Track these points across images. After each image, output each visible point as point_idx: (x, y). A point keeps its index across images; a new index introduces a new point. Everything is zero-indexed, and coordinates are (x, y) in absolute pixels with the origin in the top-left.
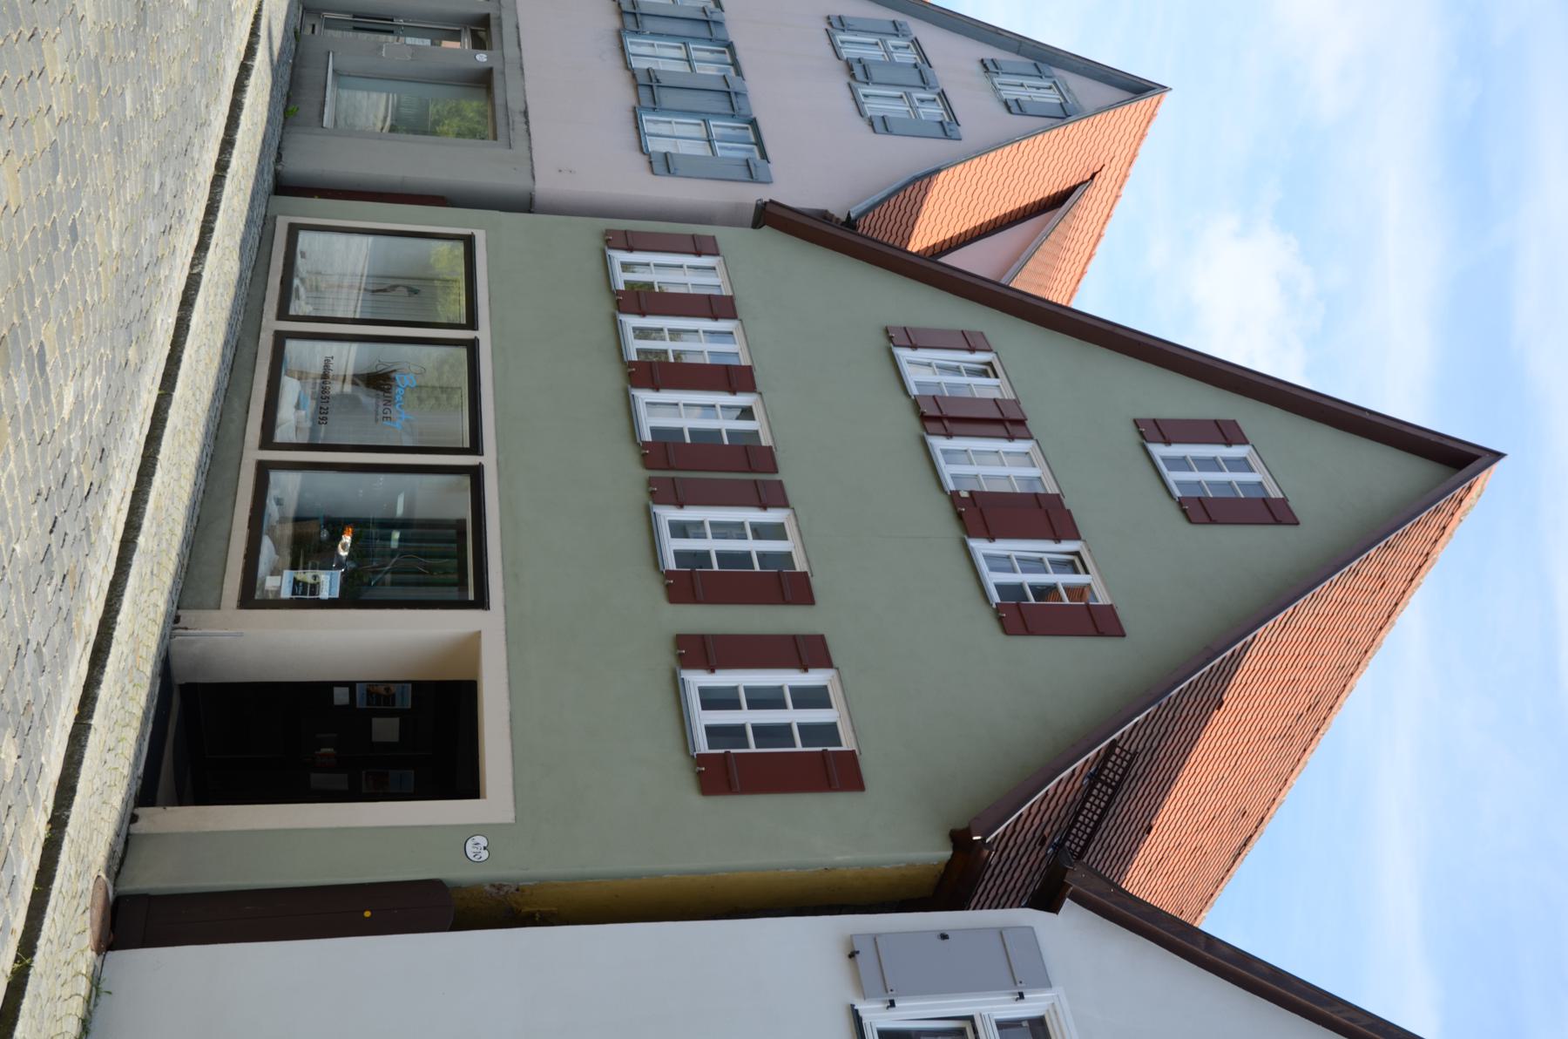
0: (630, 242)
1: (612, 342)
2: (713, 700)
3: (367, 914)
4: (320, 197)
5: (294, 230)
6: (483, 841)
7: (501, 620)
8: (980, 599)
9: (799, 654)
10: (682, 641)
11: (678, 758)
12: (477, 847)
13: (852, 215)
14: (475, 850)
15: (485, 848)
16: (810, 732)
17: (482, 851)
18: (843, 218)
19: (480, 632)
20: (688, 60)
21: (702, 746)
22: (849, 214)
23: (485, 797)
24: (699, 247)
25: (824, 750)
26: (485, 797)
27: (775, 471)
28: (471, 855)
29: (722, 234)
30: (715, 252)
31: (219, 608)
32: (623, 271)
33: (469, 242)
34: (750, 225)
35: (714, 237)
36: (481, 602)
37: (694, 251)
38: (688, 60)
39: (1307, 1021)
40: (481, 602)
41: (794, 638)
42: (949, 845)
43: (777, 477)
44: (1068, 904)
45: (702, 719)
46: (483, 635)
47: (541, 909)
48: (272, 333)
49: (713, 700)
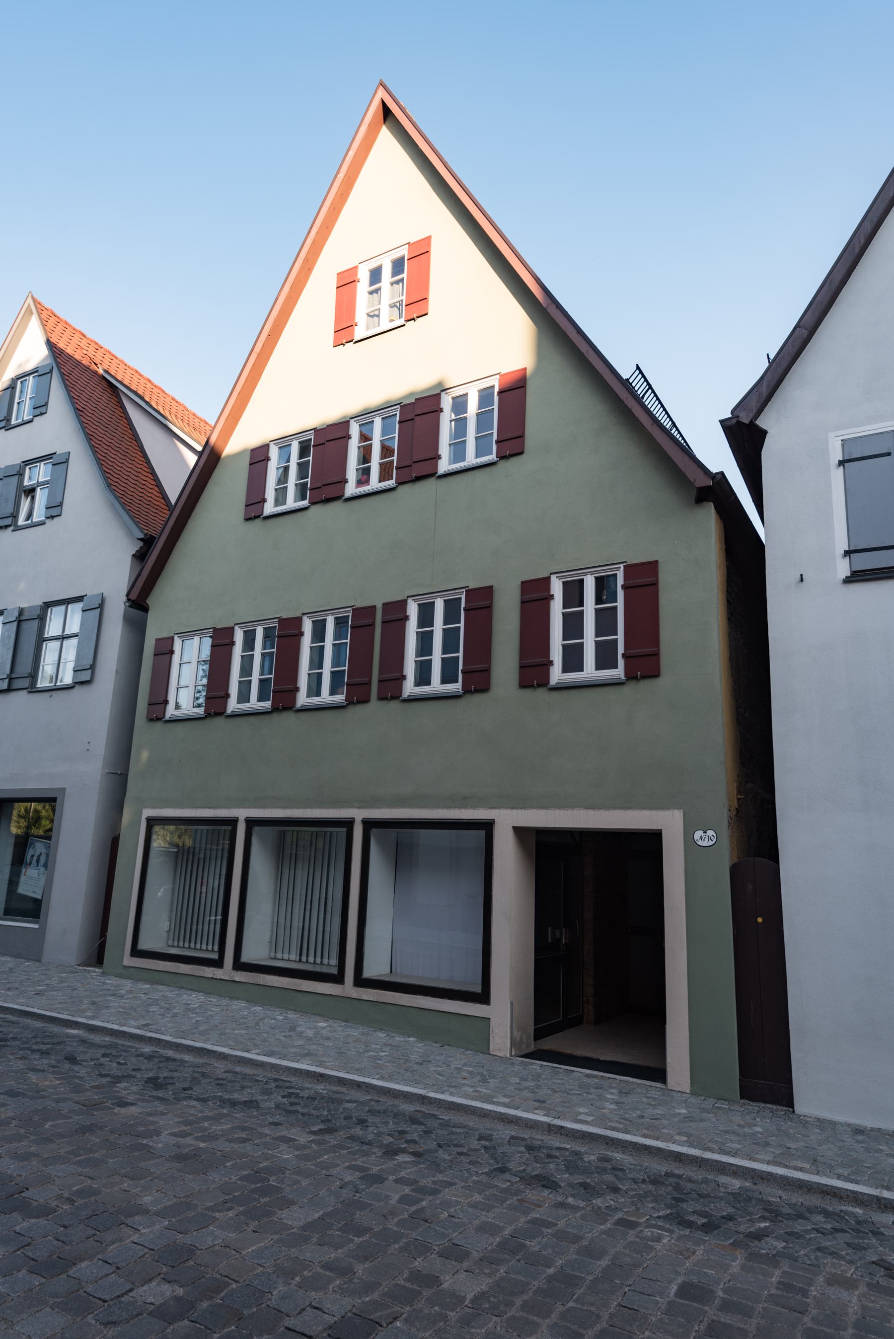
0: (159, 701)
1: (252, 719)
2: (423, 677)
3: (760, 920)
4: (106, 931)
5: (136, 952)
6: (698, 834)
7: (504, 812)
8: (493, 468)
9: (530, 601)
10: (525, 683)
11: (627, 690)
12: (704, 838)
13: (142, 536)
14: (707, 839)
15: (705, 832)
16: (451, 615)
17: (707, 834)
18: (141, 544)
19: (515, 828)
20: (63, 638)
21: (456, 687)
22: (141, 539)
23: (661, 830)
24: (165, 650)
25: (464, 610)
26: (661, 830)
27: (374, 607)
28: (711, 843)
29: (153, 632)
30: (171, 639)
31: (489, 1019)
32: (430, 685)
33: (152, 822)
34: (146, 614)
35: (156, 640)
36: (487, 827)
37: (169, 655)
38: (63, 638)
39: (852, 276)
40: (487, 827)
41: (523, 603)
42: (705, 503)
43: (379, 607)
44: (762, 422)
45: (590, 671)
46: (515, 825)
47: (736, 793)
48: (235, 971)
49: (423, 677)
